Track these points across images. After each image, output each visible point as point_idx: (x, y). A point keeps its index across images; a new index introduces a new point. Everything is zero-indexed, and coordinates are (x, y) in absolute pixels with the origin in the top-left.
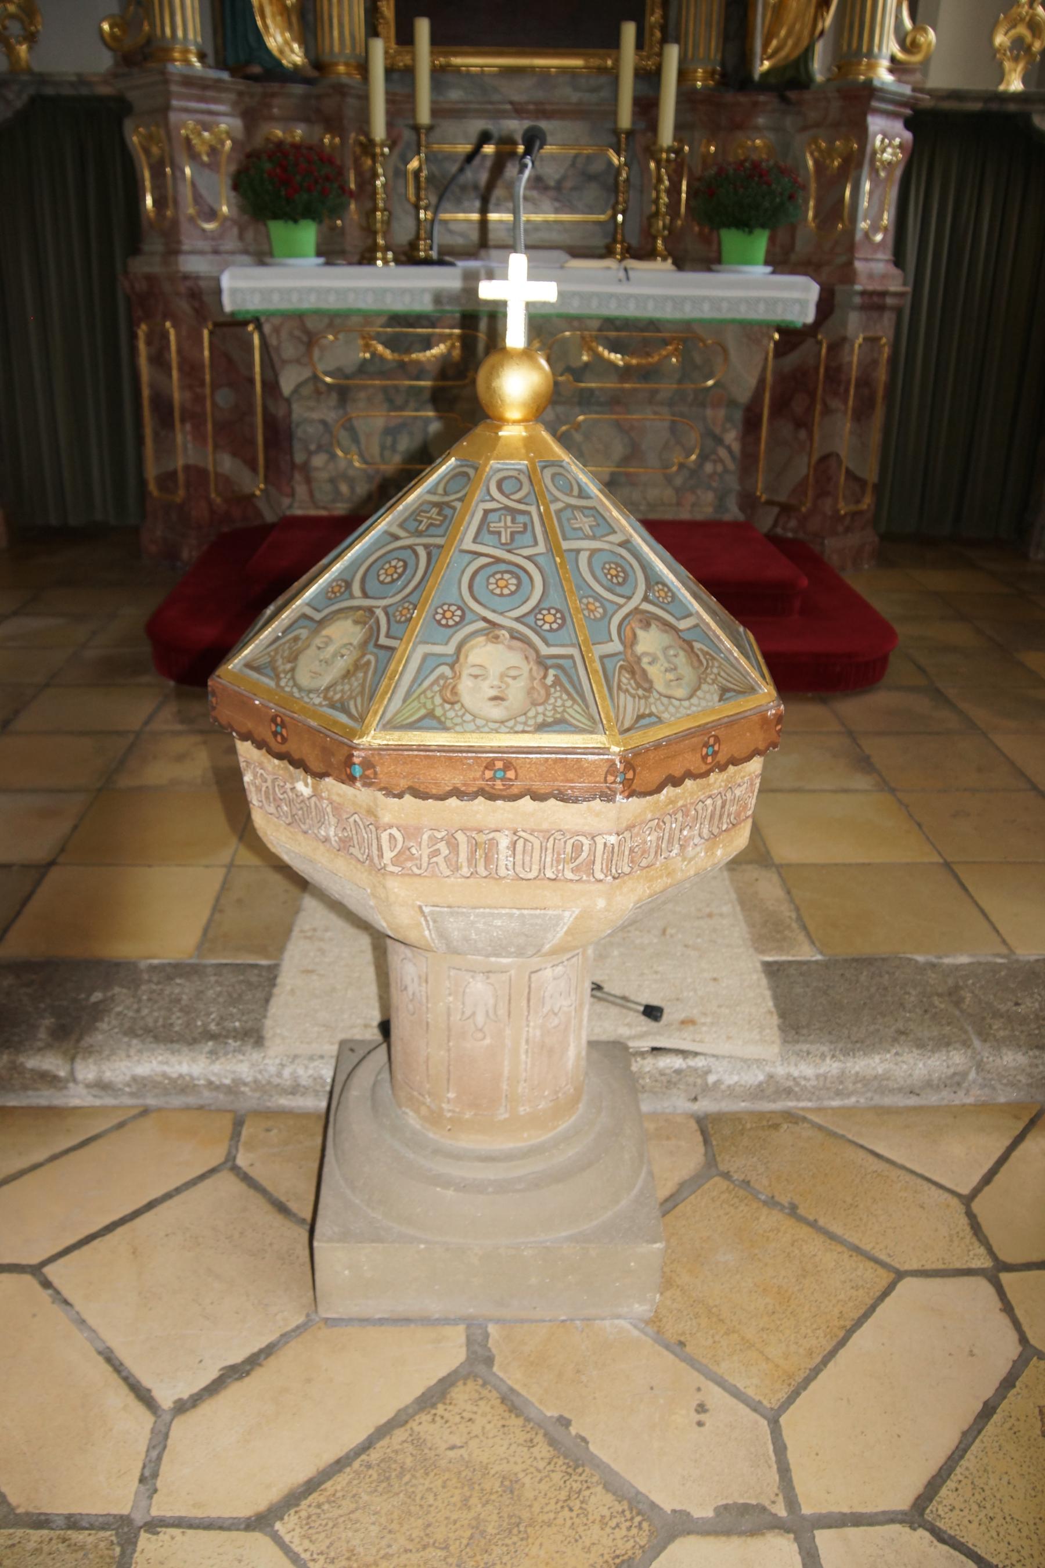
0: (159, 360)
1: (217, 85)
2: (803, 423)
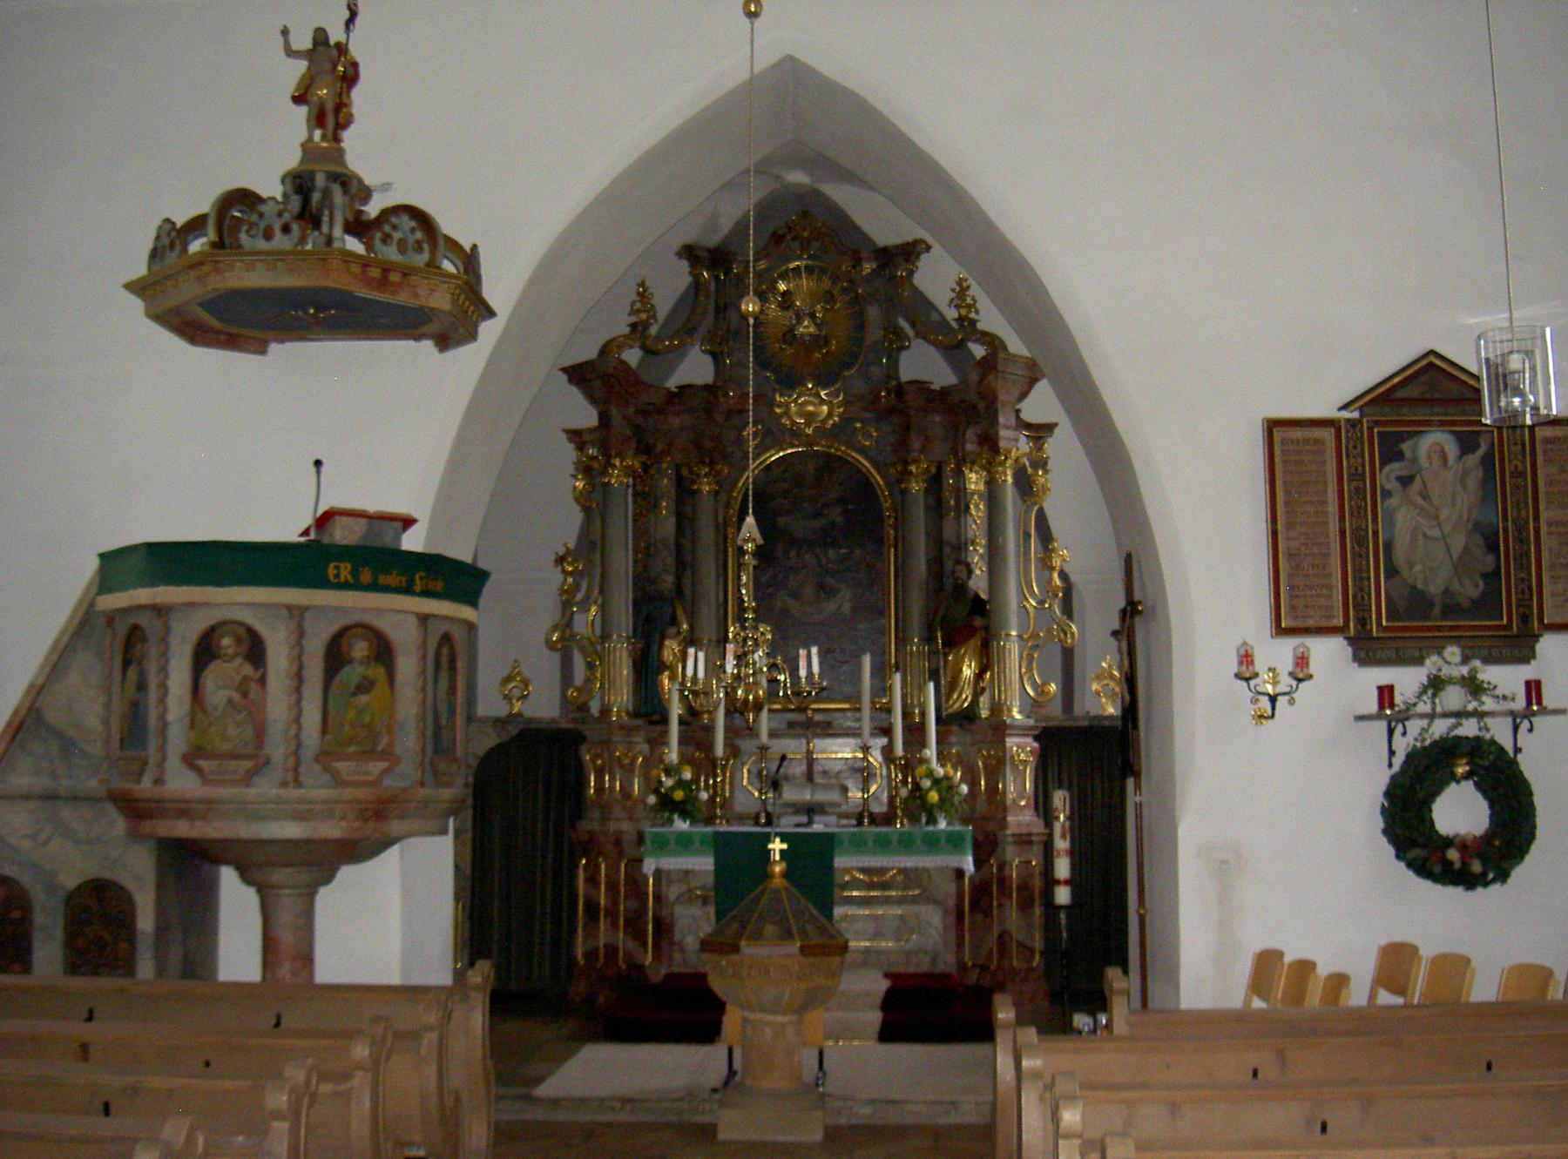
0: (592, 880)
1: (637, 728)
2: (988, 914)
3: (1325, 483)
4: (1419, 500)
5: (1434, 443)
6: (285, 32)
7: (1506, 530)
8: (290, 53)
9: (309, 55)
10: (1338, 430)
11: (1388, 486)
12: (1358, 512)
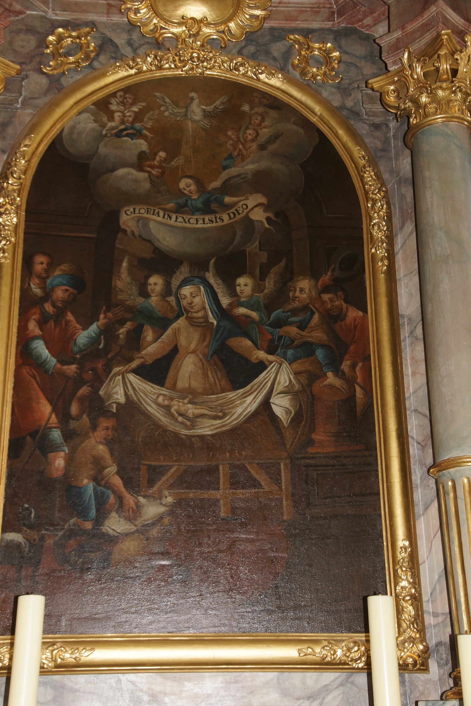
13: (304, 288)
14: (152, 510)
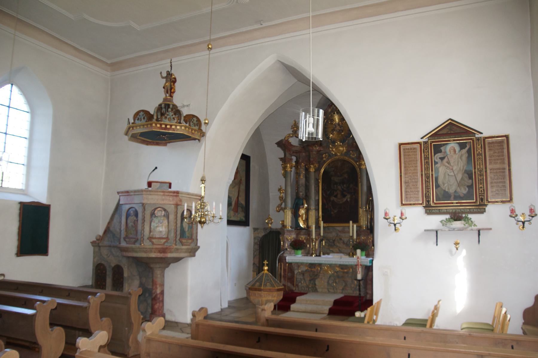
1: (292, 231)
3: (417, 161)
4: (447, 164)
5: (452, 146)
6: (161, 73)
7: (475, 173)
8: (163, 78)
9: (166, 78)
10: (421, 145)
11: (436, 161)
12: (427, 169)
13: (351, 185)
14: (336, 211)
